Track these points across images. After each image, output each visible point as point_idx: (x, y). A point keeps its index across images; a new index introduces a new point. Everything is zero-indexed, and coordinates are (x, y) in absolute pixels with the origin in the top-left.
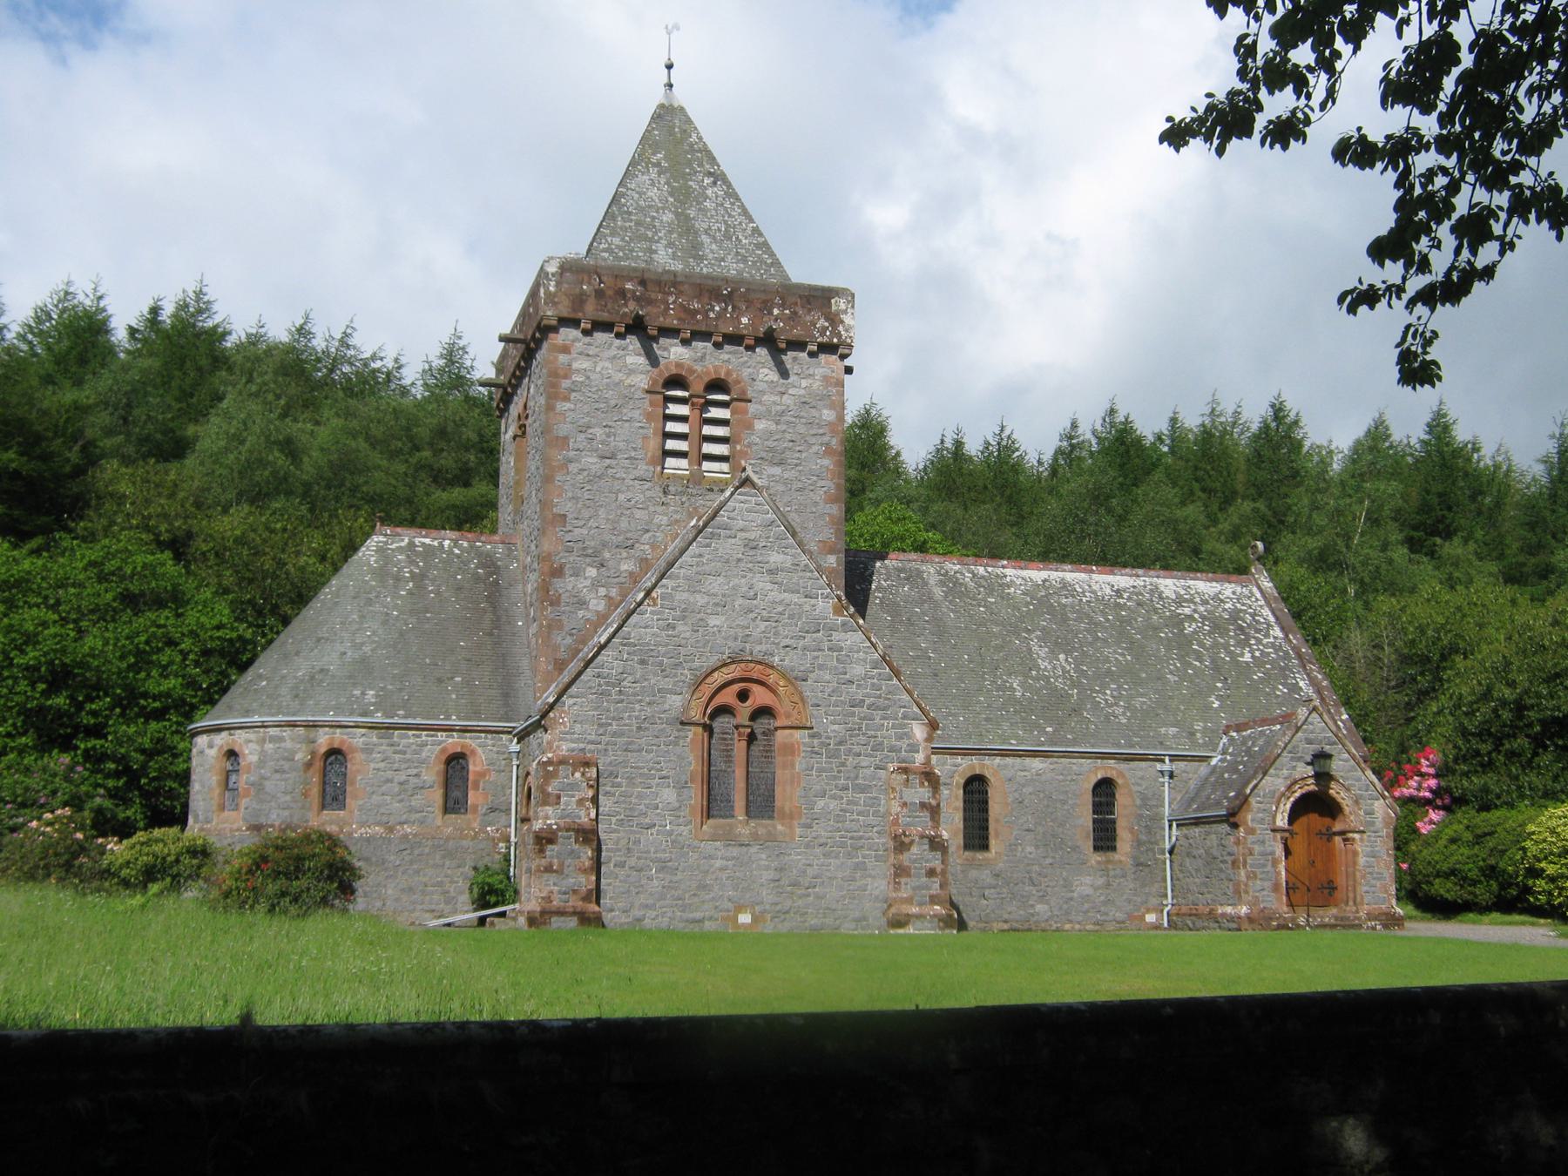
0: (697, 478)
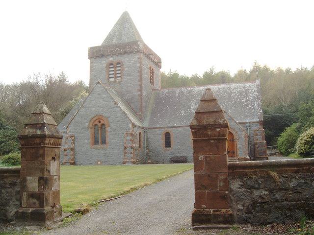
0: (115, 82)
